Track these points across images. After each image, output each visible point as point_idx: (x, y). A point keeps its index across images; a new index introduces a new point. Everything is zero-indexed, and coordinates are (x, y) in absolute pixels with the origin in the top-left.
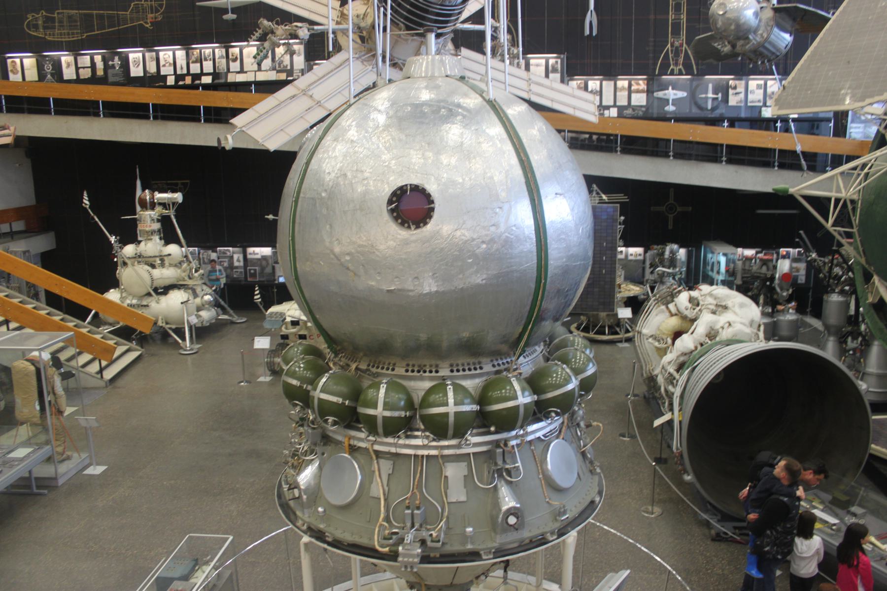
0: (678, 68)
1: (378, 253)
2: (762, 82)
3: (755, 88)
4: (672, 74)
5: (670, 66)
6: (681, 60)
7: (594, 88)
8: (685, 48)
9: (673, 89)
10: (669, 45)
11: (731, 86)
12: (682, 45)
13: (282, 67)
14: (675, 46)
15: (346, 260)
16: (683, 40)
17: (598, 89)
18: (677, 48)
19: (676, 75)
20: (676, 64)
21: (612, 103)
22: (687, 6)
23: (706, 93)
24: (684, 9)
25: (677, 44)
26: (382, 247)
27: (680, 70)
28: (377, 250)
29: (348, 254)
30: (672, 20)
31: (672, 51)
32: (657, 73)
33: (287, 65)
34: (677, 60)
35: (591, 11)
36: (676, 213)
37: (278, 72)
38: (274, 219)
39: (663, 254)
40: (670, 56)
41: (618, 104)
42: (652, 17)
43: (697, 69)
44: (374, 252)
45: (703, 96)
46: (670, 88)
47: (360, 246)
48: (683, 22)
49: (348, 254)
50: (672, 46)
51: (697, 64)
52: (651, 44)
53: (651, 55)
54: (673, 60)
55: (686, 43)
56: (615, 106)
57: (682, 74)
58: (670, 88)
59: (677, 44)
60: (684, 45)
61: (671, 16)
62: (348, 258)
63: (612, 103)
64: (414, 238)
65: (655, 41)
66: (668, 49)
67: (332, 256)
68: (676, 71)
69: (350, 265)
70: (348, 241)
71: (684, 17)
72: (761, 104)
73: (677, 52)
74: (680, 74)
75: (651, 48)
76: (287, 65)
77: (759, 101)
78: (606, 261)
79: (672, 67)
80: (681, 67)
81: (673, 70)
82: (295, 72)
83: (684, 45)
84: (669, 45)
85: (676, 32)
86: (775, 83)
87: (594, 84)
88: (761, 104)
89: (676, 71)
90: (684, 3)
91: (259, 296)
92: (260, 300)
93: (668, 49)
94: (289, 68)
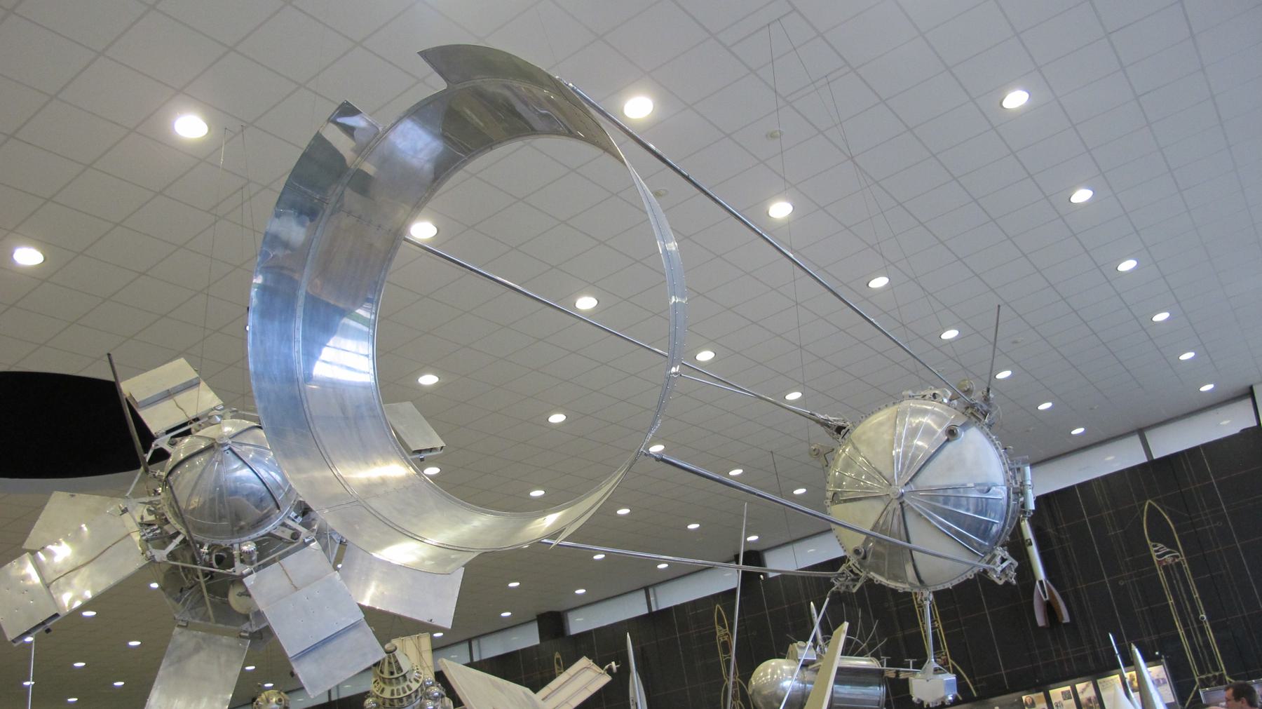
2: (1068, 688)
3: (1061, 699)
8: (952, 665)
11: (1026, 702)
16: (946, 655)
22: (938, 609)
43: (977, 690)
48: (940, 631)
55: (951, 659)
60: (950, 660)
83: (950, 660)
86: (1087, 686)
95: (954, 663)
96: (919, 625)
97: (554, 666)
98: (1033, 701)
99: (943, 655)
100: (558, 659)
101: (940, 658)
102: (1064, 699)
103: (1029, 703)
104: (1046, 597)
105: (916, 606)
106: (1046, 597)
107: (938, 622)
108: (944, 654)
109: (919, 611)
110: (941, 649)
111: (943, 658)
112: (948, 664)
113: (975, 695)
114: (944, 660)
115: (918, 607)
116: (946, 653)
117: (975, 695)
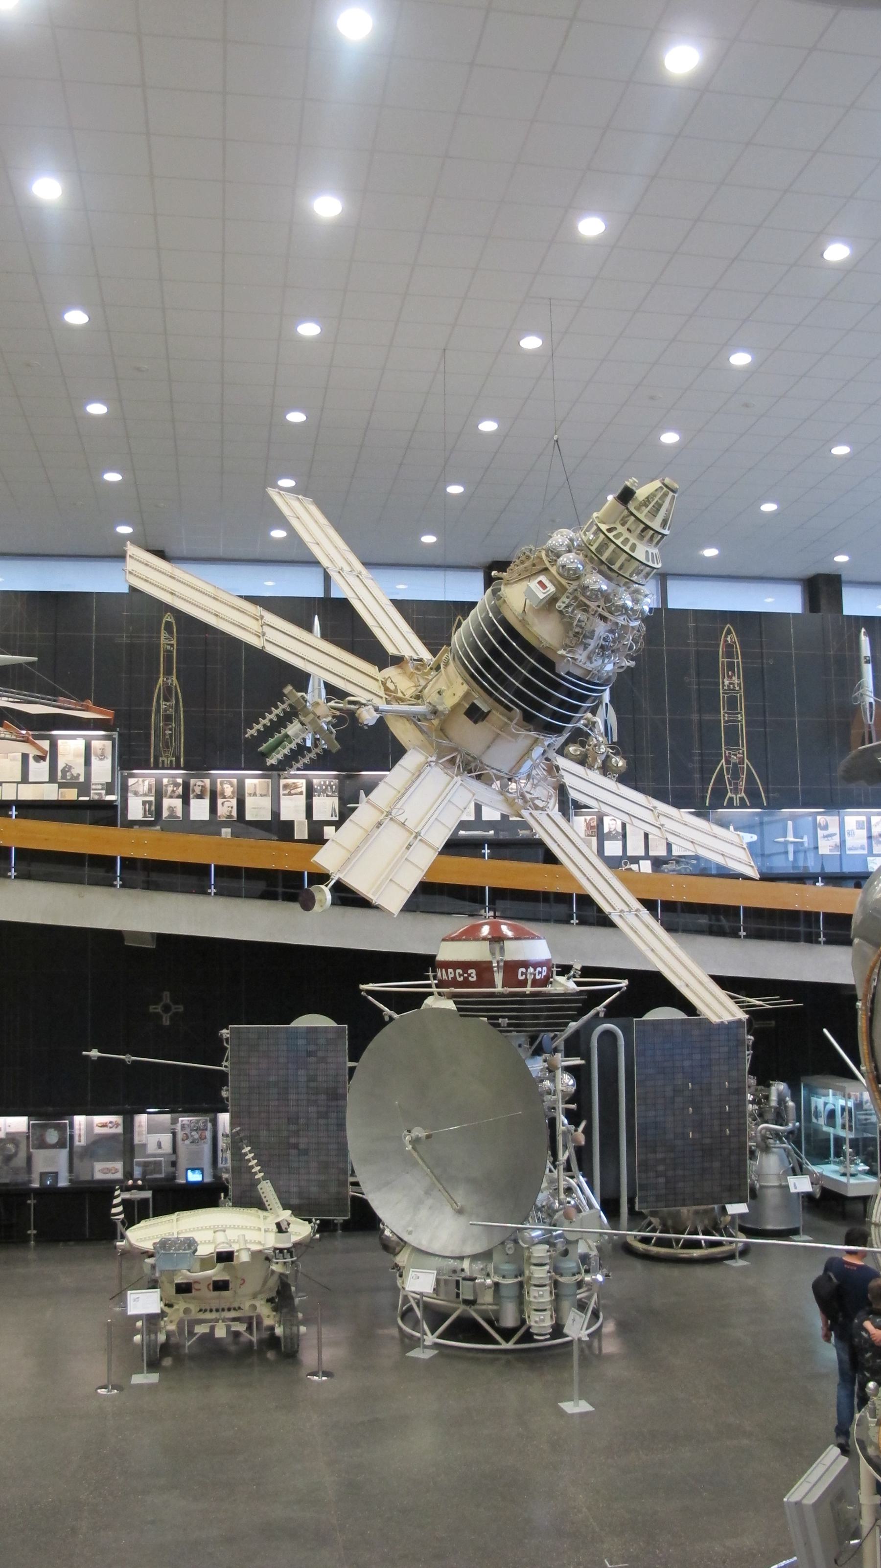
2: (863, 818)
3: (854, 827)
4: (731, 805)
6: (742, 785)
7: (613, 827)
8: (747, 765)
10: (723, 761)
11: (820, 823)
12: (742, 761)
13: (68, 778)
14: (732, 761)
16: (743, 753)
17: (620, 830)
18: (735, 765)
19: (737, 807)
20: (736, 791)
21: (642, 853)
23: (785, 836)
24: (742, 704)
25: (734, 759)
27: (742, 799)
30: (725, 722)
31: (728, 769)
32: (707, 804)
33: (79, 775)
34: (736, 784)
35: (607, 704)
37: (62, 786)
38: (99, 1058)
39: (767, 1098)
40: (726, 777)
41: (651, 853)
42: (695, 717)
43: (767, 798)
45: (782, 840)
48: (742, 725)
50: (728, 762)
51: (767, 791)
52: (697, 758)
53: (697, 776)
54: (730, 785)
55: (747, 759)
56: (647, 857)
57: (746, 807)
59: (734, 759)
60: (746, 761)
61: (724, 716)
63: (642, 853)
65: (701, 755)
66: (722, 765)
68: (736, 802)
71: (742, 718)
72: (865, 852)
73: (736, 772)
74: (743, 805)
75: (697, 765)
76: (79, 775)
77: (862, 848)
78: (729, 1113)
79: (729, 795)
80: (743, 795)
81: (731, 799)
82: (93, 787)
83: (746, 761)
84: (723, 761)
87: (613, 822)
88: (865, 852)
89: (736, 802)
90: (741, 696)
91: (120, 1209)
92: (122, 1216)
93: (722, 765)
94: (82, 779)
95: (749, 764)
97: (159, 632)
98: (827, 822)
99: (739, 753)
100: (168, 624)
101: (735, 755)
102: (857, 829)
104: (871, 721)
105: (721, 691)
106: (871, 721)
107: (742, 716)
108: (741, 751)
109: (724, 697)
111: (738, 755)
112: (743, 764)
114: (740, 758)
115: (723, 693)
116: (743, 751)
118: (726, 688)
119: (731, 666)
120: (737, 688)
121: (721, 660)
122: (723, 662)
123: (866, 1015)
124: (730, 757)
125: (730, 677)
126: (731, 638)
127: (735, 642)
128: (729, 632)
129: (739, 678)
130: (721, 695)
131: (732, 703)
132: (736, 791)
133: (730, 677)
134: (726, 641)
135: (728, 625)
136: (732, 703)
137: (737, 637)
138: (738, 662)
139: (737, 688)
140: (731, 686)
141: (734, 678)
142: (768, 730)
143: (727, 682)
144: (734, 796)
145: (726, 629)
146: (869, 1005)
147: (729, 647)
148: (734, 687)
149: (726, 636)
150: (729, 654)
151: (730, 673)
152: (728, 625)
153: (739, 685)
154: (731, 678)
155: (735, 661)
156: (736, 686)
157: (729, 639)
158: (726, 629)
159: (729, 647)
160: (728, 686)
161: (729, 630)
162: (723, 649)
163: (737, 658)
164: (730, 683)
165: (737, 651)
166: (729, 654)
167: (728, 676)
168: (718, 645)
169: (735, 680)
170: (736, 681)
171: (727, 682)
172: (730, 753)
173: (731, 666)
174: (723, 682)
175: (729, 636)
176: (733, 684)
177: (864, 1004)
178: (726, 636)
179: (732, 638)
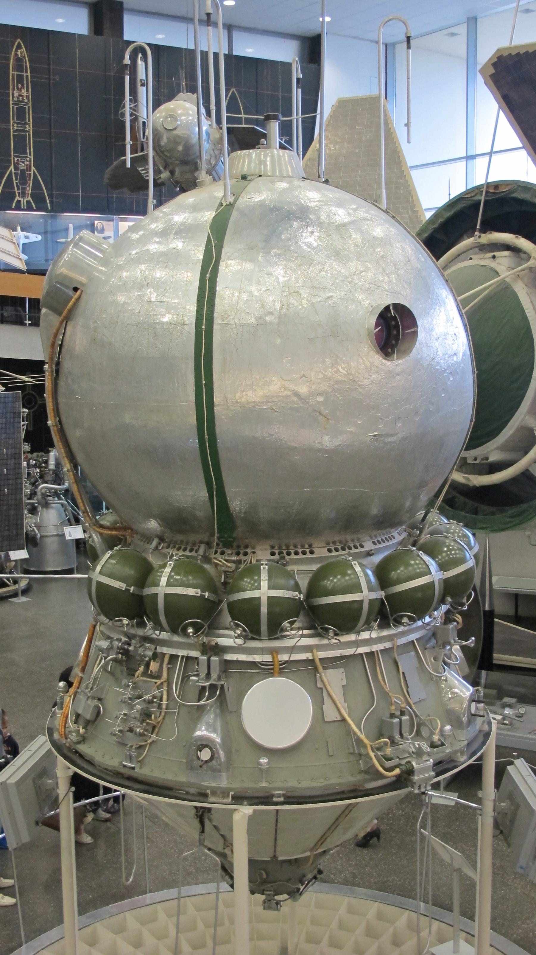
0: (26, 200)
1: (361, 390)
4: (18, 208)
5: (15, 196)
6: (29, 190)
8: (34, 172)
9: (22, 230)
10: (12, 167)
11: (97, 227)
12: (29, 168)
14: (21, 168)
15: (318, 402)
16: (30, 161)
18: (23, 171)
19: (24, 210)
20: (23, 195)
24: (30, 116)
25: (22, 166)
26: (365, 382)
27: (28, 202)
28: (359, 385)
29: (320, 394)
30: (14, 131)
31: (16, 174)
34: (24, 189)
36: (36, 408)
40: (15, 181)
43: (51, 202)
44: (356, 389)
46: (19, 228)
47: (338, 382)
48: (29, 135)
49: (320, 394)
50: (16, 168)
51: (51, 196)
54: (18, 189)
55: (34, 166)
58: (19, 228)
59: (22, 166)
60: (33, 168)
61: (13, 126)
62: (321, 399)
64: (398, 369)
66: (11, 172)
67: (295, 399)
68: (24, 205)
69: (322, 408)
70: (321, 376)
71: (29, 128)
73: (23, 177)
74: (29, 208)
79: (17, 198)
80: (29, 198)
81: (19, 202)
83: (33, 168)
84: (12, 167)
85: (21, 150)
89: (24, 205)
90: (29, 108)
93: (11, 172)
95: (35, 171)
96: (10, 123)
98: (103, 227)
99: (27, 161)
101: (23, 162)
103: (99, 229)
105: (11, 102)
106: (144, 138)
107: (29, 126)
108: (28, 159)
109: (13, 108)
110: (26, 153)
111: (26, 163)
112: (30, 171)
113: (50, 209)
114: (27, 165)
115: (13, 104)
116: (30, 159)
117: (50, 209)
118: (15, 99)
119: (20, 79)
120: (26, 101)
121: (11, 72)
122: (13, 75)
123: (52, 375)
124: (18, 164)
125: (19, 90)
126: (21, 53)
127: (24, 57)
128: (19, 47)
129: (27, 91)
130: (11, 106)
131: (21, 114)
132: (23, 195)
133: (19, 90)
134: (16, 55)
135: (19, 40)
136: (21, 114)
137: (27, 52)
138: (27, 76)
139: (26, 101)
140: (21, 98)
141: (23, 91)
142: (53, 141)
143: (16, 94)
144: (22, 200)
145: (16, 44)
146: (54, 367)
147: (19, 61)
148: (23, 99)
149: (16, 51)
150: (19, 67)
151: (20, 86)
152: (19, 40)
153: (28, 97)
154: (21, 91)
155: (25, 74)
156: (25, 98)
157: (19, 53)
158: (16, 44)
159: (19, 61)
160: (18, 98)
161: (19, 45)
162: (13, 62)
163: (27, 72)
164: (20, 95)
165: (26, 66)
166: (19, 67)
167: (18, 89)
168: (8, 59)
169: (24, 92)
170: (25, 94)
171: (16, 94)
172: (18, 160)
173: (20, 79)
174: (13, 94)
175: (19, 51)
176: (22, 96)
177: (51, 367)
178: (16, 51)
179: (22, 52)
